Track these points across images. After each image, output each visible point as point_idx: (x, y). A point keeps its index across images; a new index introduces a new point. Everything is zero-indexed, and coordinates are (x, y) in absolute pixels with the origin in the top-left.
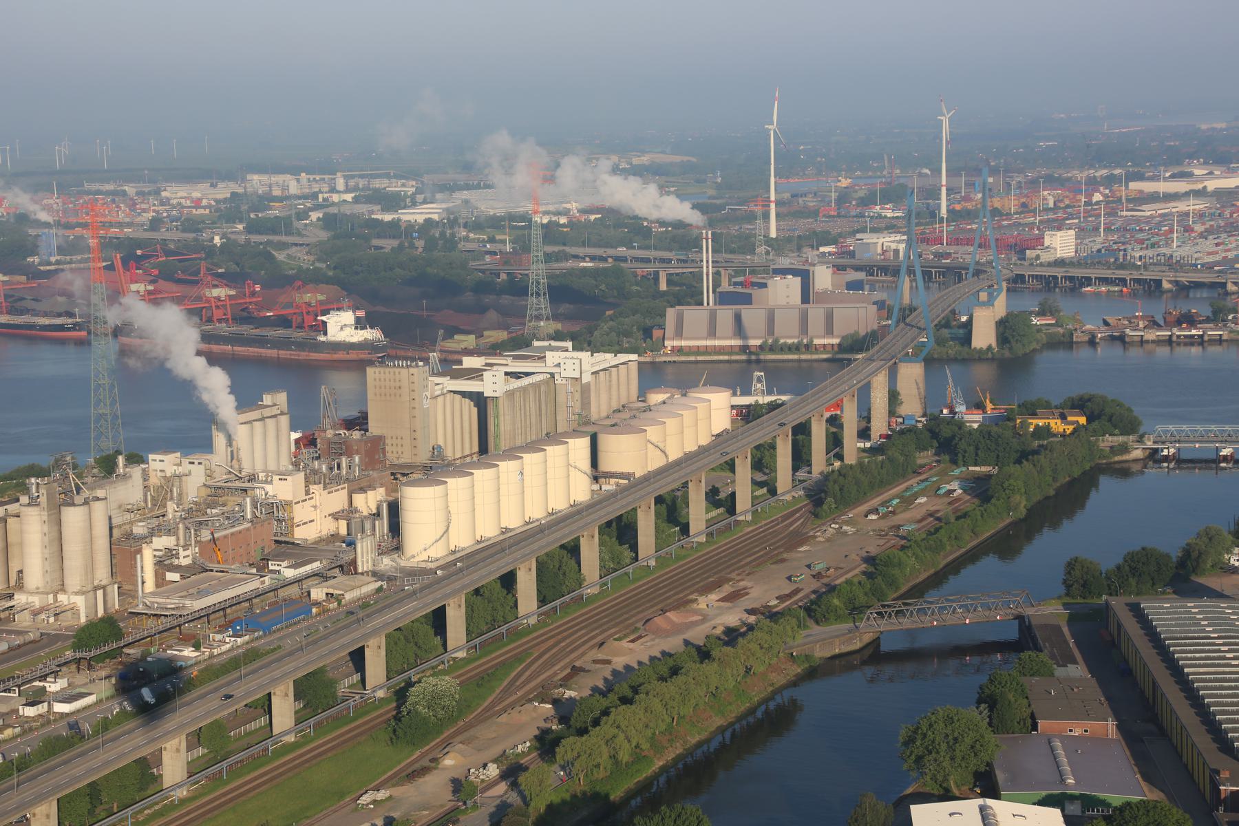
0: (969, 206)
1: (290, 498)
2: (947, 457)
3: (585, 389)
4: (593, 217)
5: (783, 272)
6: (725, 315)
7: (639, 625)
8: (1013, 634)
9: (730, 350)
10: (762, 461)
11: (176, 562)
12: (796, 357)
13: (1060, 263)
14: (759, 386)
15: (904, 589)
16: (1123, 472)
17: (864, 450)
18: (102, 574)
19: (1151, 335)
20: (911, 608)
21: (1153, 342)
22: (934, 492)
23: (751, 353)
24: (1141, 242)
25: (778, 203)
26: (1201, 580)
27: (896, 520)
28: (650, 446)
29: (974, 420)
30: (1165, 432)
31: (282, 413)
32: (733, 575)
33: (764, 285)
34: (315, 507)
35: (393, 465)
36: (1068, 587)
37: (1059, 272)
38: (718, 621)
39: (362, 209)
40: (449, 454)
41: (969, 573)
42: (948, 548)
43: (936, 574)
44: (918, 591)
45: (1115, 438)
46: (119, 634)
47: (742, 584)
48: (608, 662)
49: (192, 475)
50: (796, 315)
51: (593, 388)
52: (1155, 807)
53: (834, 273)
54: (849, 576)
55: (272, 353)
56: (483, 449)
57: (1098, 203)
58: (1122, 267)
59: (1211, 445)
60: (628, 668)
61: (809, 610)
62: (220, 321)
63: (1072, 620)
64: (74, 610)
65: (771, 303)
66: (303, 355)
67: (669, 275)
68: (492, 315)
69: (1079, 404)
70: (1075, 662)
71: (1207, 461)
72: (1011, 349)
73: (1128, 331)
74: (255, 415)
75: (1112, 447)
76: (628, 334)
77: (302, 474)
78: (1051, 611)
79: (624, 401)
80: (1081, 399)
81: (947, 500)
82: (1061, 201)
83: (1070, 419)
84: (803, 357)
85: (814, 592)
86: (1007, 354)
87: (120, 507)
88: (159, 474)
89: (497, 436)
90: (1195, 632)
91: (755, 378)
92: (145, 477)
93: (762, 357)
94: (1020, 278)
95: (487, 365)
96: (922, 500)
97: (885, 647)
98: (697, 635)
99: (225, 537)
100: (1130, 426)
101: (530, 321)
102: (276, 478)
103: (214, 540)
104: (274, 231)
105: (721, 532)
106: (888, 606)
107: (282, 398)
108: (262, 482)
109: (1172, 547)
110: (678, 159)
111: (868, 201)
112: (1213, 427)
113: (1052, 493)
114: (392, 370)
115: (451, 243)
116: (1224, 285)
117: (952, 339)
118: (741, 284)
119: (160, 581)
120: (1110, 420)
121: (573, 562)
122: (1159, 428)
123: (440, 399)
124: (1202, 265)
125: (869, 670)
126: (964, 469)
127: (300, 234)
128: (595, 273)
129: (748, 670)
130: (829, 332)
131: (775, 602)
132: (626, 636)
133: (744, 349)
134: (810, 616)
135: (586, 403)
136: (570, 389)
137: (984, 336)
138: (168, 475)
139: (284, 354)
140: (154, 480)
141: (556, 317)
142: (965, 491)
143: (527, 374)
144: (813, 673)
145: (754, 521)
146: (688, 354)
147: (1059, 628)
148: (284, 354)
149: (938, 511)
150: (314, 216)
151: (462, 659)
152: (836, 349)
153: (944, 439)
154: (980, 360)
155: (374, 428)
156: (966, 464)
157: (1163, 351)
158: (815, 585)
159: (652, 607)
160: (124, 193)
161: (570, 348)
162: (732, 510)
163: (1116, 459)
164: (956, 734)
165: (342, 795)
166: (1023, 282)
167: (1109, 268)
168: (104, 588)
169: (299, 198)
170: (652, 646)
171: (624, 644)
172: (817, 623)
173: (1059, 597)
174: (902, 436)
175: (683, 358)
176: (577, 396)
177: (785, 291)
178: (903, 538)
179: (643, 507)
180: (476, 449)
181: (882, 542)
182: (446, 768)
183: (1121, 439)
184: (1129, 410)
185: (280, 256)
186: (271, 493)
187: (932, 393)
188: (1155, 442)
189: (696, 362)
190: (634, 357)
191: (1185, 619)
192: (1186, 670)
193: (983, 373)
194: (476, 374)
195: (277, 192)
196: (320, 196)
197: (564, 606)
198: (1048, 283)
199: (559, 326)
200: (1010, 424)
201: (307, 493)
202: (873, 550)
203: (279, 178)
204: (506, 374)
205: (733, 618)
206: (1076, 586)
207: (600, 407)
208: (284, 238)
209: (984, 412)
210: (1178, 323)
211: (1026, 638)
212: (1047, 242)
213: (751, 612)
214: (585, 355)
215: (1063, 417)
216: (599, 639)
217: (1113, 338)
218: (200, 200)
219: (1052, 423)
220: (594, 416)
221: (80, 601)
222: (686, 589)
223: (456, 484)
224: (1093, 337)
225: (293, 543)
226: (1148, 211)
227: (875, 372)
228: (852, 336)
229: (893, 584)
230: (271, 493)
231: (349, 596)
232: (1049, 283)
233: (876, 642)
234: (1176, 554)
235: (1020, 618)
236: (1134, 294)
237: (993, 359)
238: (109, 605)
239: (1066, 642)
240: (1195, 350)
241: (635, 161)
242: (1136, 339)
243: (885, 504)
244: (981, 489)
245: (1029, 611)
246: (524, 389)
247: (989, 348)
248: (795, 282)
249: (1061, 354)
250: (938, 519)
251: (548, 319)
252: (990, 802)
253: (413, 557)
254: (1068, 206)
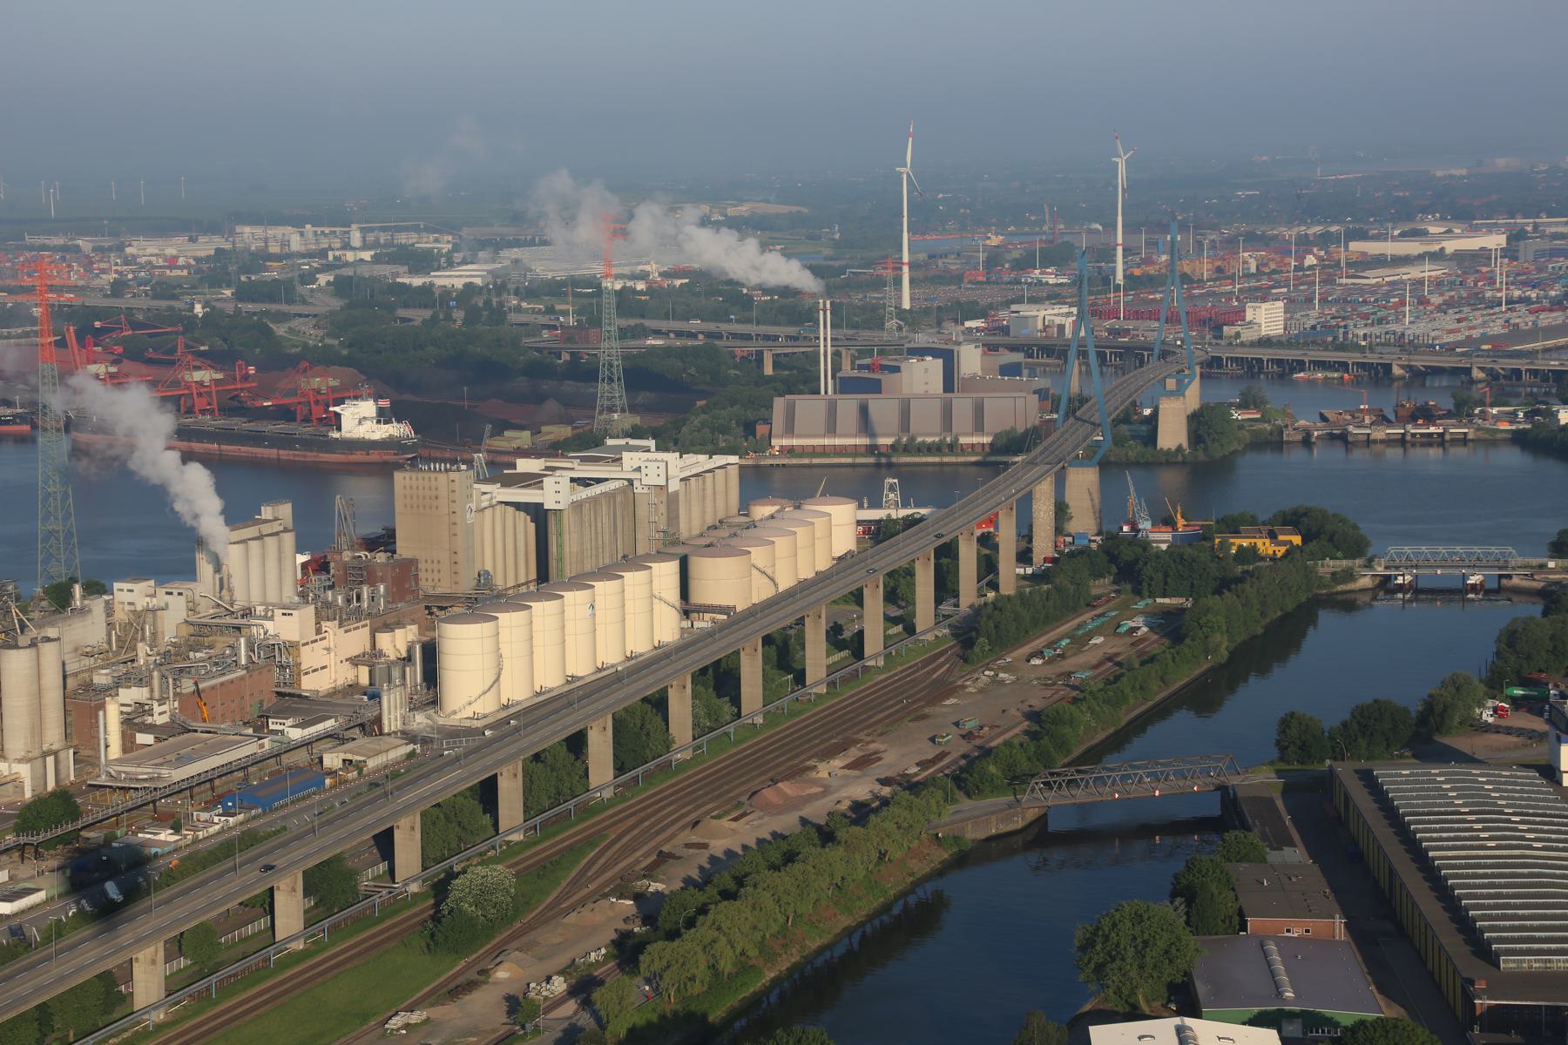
0: (1151, 270)
1: (295, 637)
2: (1128, 587)
3: (672, 500)
4: (678, 283)
5: (921, 352)
6: (848, 406)
7: (744, 799)
8: (1215, 810)
9: (854, 451)
10: (897, 591)
11: (149, 720)
12: (937, 459)
13: (1265, 342)
14: (892, 496)
15: (1077, 751)
16: (1348, 605)
17: (1025, 577)
18: (53, 735)
19: (1379, 433)
20: (1087, 777)
21: (1382, 441)
22: (1112, 629)
23: (880, 455)
24: (1365, 316)
25: (912, 265)
26: (1446, 741)
27: (1066, 665)
28: (754, 572)
29: (1162, 539)
30: (1399, 555)
31: (286, 530)
32: (861, 736)
33: (897, 369)
34: (328, 649)
35: (427, 597)
36: (1283, 750)
37: (1265, 354)
38: (844, 793)
39: (385, 270)
40: (499, 582)
41: (1157, 732)
42: (1132, 701)
43: (1116, 733)
44: (1094, 756)
45: (1338, 562)
46: (75, 813)
47: (873, 746)
48: (705, 846)
49: (174, 610)
50: (937, 404)
51: (682, 497)
52: (1395, 1027)
53: (984, 353)
54: (1007, 736)
55: (272, 453)
56: (543, 575)
57: (1311, 267)
58: (1342, 347)
59: (1456, 572)
60: (729, 853)
61: (957, 780)
62: (203, 412)
63: (1287, 791)
64: (16, 782)
65: (906, 391)
66: (311, 456)
67: (776, 356)
68: (552, 406)
69: (1293, 520)
70: (1292, 844)
71: (1451, 591)
72: (1206, 450)
73: (1351, 428)
74: (251, 532)
75: (1333, 574)
76: (724, 430)
77: (310, 610)
78: (1261, 780)
79: (721, 515)
80: (1295, 513)
81: (1129, 640)
82: (1266, 265)
83: (1281, 538)
84: (946, 459)
85: (964, 756)
86: (1201, 456)
87: (76, 650)
88: (127, 608)
89: (560, 560)
90: (1440, 805)
91: (886, 486)
92: (109, 610)
93: (894, 460)
94: (1216, 361)
95: (547, 468)
96: (1098, 640)
97: (1052, 827)
98: (817, 811)
99: (213, 688)
100: (1356, 547)
101: (601, 413)
102: (278, 612)
103: (198, 692)
104: (272, 298)
105: (844, 681)
106: (1058, 774)
107: (285, 510)
108: (260, 617)
109: (1411, 699)
110: (784, 209)
111: (1025, 264)
112: (1458, 549)
113: (1260, 631)
114: (427, 475)
115: (498, 315)
116: (1468, 371)
117: (1133, 438)
118: (867, 367)
119: (128, 744)
120: (1331, 540)
121: (659, 719)
122: (1392, 550)
123: (488, 513)
124: (1441, 346)
125: (1034, 857)
126: (1150, 601)
127: (304, 302)
128: (683, 353)
129: (882, 855)
130: (979, 428)
131: (915, 770)
132: (726, 813)
133: (872, 449)
134: (959, 788)
135: (673, 517)
136: (654, 499)
137: (1172, 435)
138: (139, 608)
139: (285, 454)
140: (120, 615)
141: (633, 409)
142: (1151, 629)
143: (599, 481)
144: (963, 859)
145: (887, 667)
146: (801, 456)
147: (1271, 801)
148: (285, 454)
149: (1117, 654)
150: (323, 279)
151: (517, 843)
152: (987, 449)
153: (1124, 563)
154: (1168, 464)
155: (404, 549)
156: (1152, 595)
157: (1394, 453)
158: (965, 747)
159: (759, 776)
160: (78, 249)
161: (653, 448)
162: (859, 653)
163: (1340, 588)
164: (1146, 936)
165: (365, 1017)
166: (1220, 366)
167: (1326, 349)
168: (56, 753)
169: (303, 256)
170: (759, 827)
171: (725, 823)
172: (969, 796)
173: (1271, 763)
174: (1072, 560)
175: (794, 461)
176: (663, 509)
177: (923, 376)
178: (1074, 688)
179: (748, 650)
180: (533, 576)
181: (1048, 693)
182: (498, 983)
183: (1345, 563)
184: (1355, 527)
185: (280, 330)
186: (271, 632)
187: (1109, 506)
188: (1386, 568)
190: (734, 459)
191: (1428, 789)
192: (1431, 854)
193: (1171, 479)
194: (533, 480)
195: (274, 249)
196: (331, 254)
197: (648, 776)
198: (1251, 367)
199: (637, 420)
200: (1207, 544)
201: (318, 631)
202: (1037, 704)
203: (278, 231)
204: (573, 480)
205: (861, 790)
206: (1292, 748)
207: (691, 523)
208: (284, 308)
209: (1175, 529)
210: (1413, 418)
211: (1229, 815)
212: (1249, 317)
213: (884, 782)
214: (672, 457)
215: (1272, 536)
216: (693, 816)
217: (1332, 437)
218: (175, 258)
219: (1259, 543)
220: (684, 532)
221: (24, 771)
222: (802, 753)
223: (509, 621)
224: (1308, 435)
225: (300, 696)
226: (1373, 278)
227: (1039, 479)
228: (1007, 433)
229: (1063, 746)
230: (271, 632)
231: (372, 763)
232: (1252, 368)
233: (1042, 820)
234: (1415, 707)
235: (1222, 789)
236: (1357, 382)
237: (1184, 463)
238: (63, 776)
239: (1280, 819)
240: (1434, 452)
241: (731, 211)
242: (1361, 438)
243: (1051, 645)
244: (1171, 626)
245: (1234, 781)
246: (594, 500)
247: (1180, 448)
248: (935, 366)
249: (1268, 457)
250: (1119, 664)
251: (623, 410)
252: (1189, 1021)
253: (455, 713)
254: (1274, 272)
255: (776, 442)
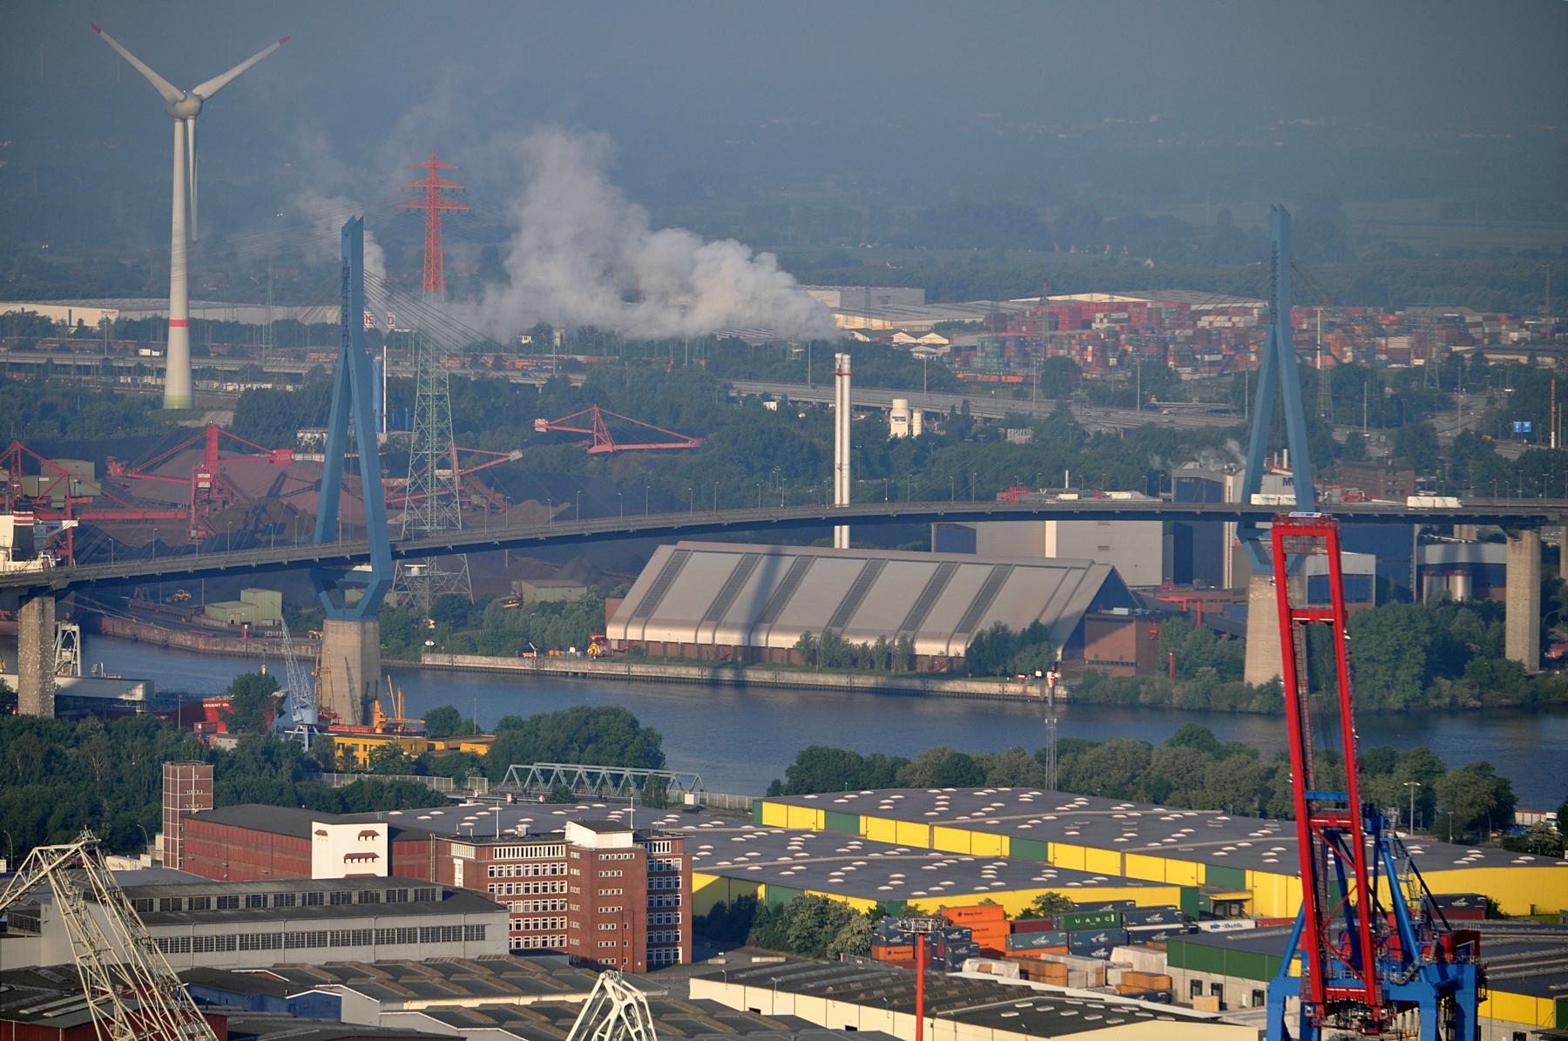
14: (67, 655)
189: (629, 679)
255: (614, 632)
